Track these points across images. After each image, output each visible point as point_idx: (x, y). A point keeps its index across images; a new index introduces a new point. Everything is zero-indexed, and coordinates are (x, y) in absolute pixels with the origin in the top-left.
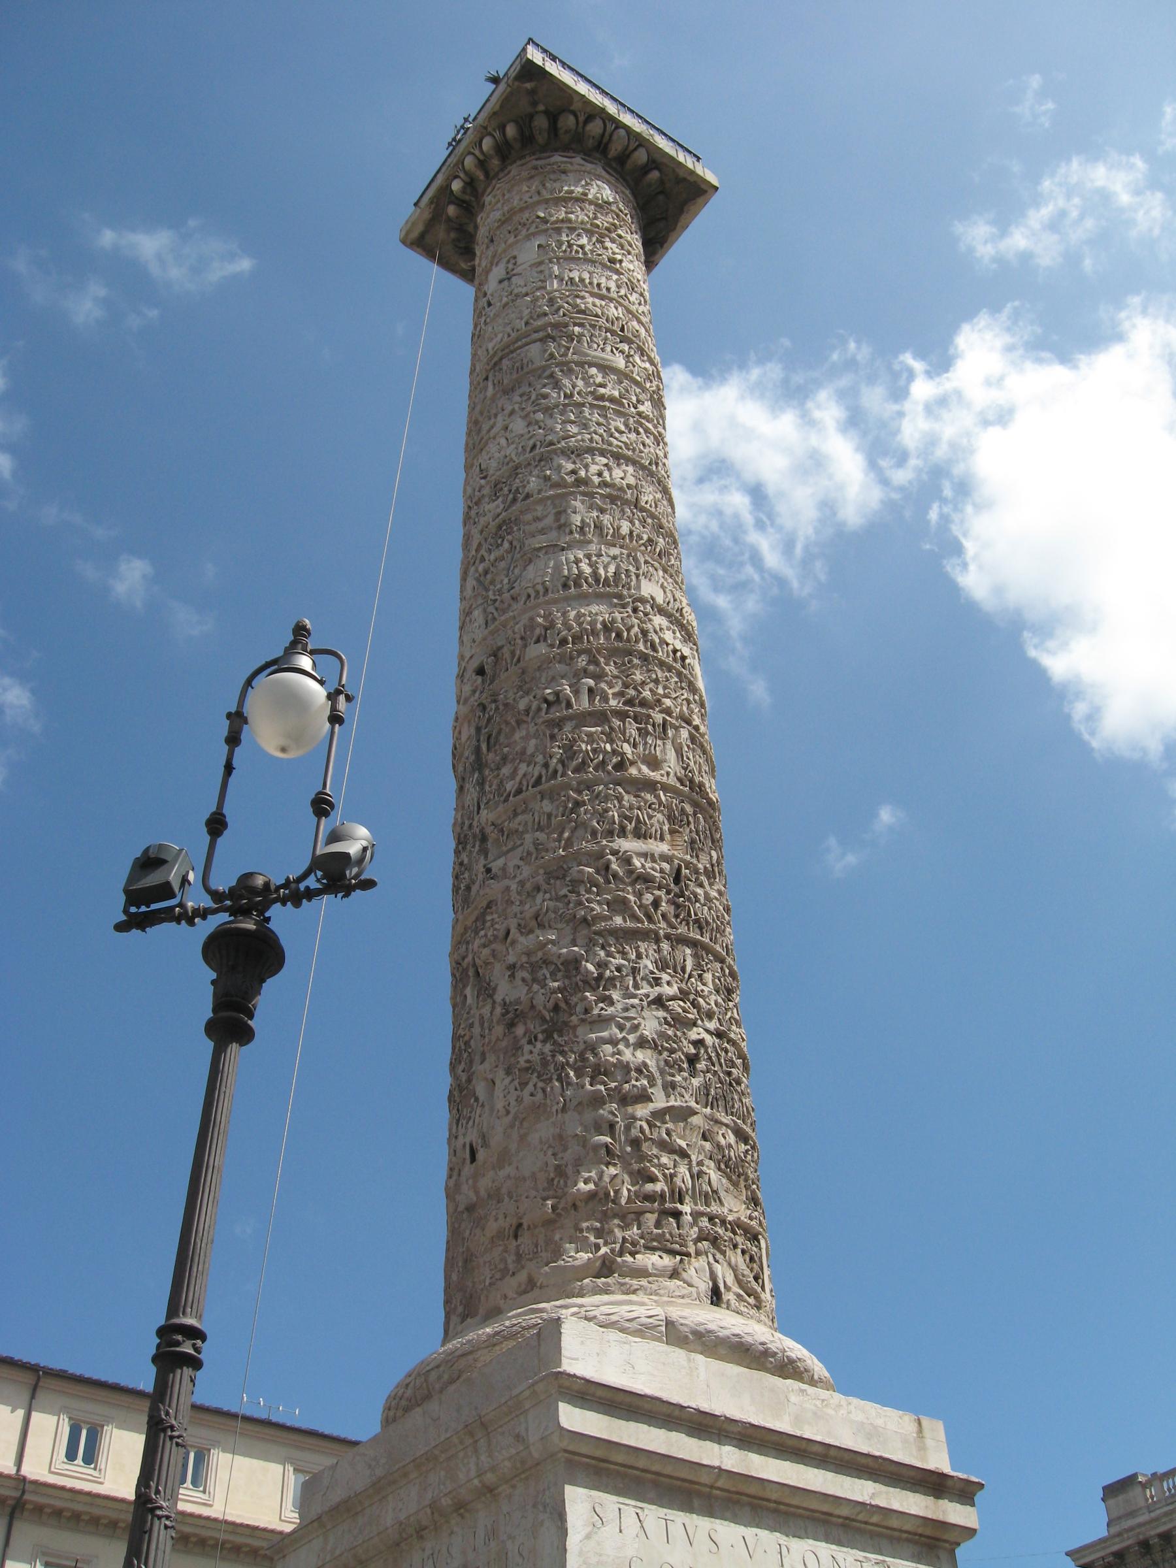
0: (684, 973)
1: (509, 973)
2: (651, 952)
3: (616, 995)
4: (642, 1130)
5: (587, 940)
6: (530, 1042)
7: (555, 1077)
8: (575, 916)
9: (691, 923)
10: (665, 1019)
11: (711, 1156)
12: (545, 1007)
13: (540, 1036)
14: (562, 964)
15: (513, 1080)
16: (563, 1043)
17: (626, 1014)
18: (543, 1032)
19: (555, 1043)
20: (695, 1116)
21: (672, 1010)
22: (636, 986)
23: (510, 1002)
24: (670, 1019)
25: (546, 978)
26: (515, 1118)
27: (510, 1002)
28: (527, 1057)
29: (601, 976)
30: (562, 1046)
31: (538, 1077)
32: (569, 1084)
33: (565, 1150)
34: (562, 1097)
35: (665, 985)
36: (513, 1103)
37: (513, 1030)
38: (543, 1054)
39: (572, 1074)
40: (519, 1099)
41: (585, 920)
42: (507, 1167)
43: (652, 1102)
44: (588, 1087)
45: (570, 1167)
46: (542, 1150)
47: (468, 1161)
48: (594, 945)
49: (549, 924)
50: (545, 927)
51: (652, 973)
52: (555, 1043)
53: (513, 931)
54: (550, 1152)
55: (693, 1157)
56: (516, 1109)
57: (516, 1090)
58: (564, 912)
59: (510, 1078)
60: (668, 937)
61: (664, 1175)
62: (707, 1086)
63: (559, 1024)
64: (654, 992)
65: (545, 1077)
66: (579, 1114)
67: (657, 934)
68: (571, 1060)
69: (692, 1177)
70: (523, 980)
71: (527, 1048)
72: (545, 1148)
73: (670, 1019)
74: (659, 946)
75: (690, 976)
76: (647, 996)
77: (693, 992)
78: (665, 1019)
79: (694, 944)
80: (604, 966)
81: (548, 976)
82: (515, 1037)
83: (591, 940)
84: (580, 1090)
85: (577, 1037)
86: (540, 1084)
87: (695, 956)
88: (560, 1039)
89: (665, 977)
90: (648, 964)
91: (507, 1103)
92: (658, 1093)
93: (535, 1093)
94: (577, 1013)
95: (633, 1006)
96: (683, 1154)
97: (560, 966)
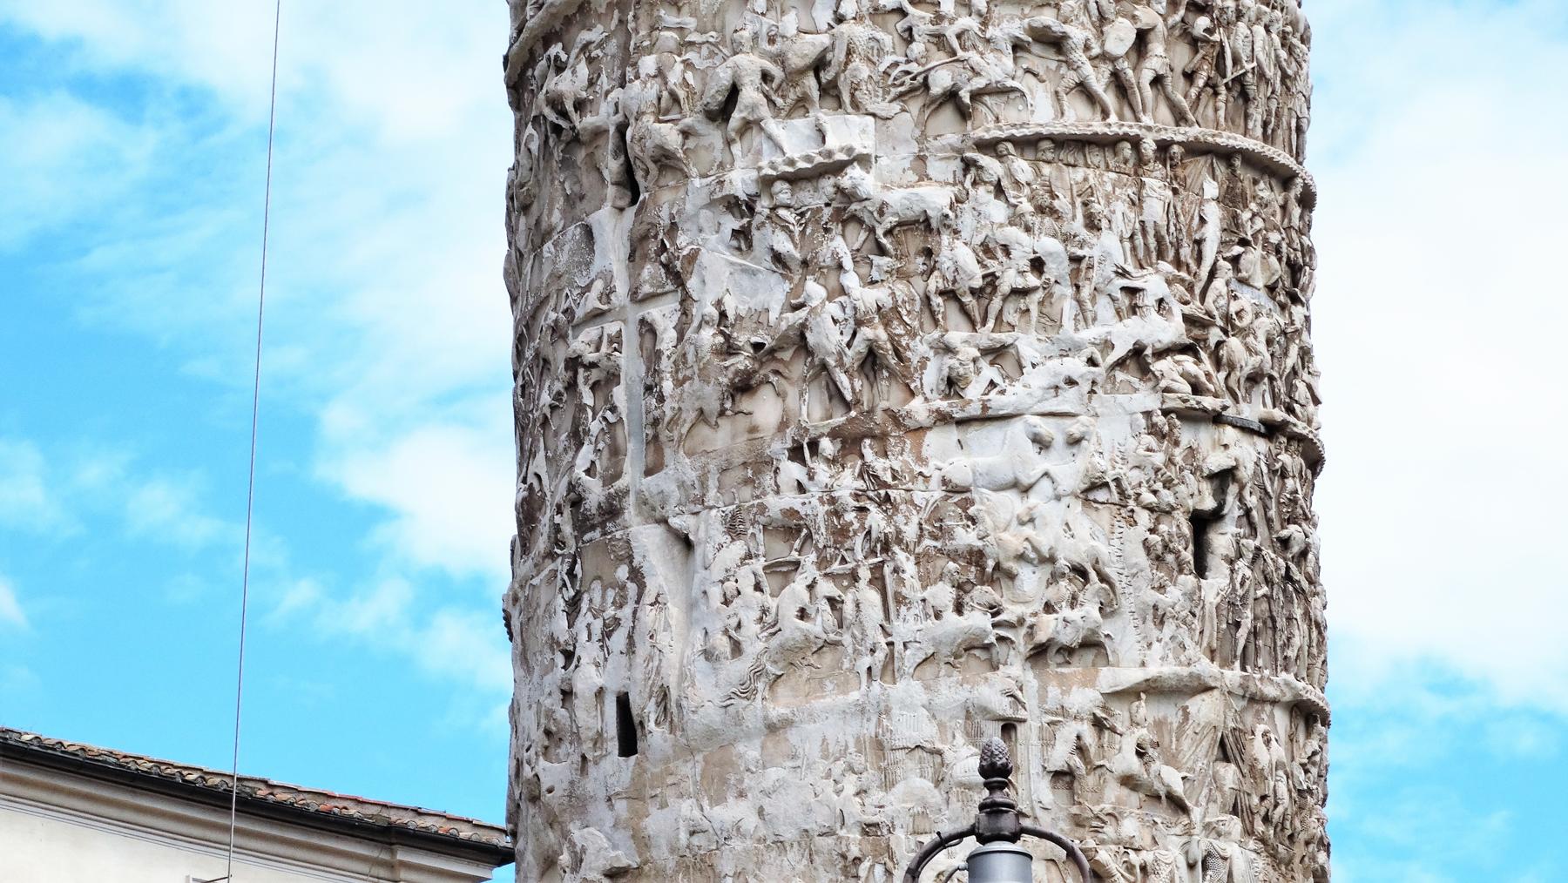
0: (1199, 259)
1: (737, 225)
2: (1121, 207)
3: (1028, 344)
4: (1081, 749)
5: (957, 165)
6: (796, 454)
7: (865, 574)
8: (926, 85)
9: (1223, 90)
10: (1148, 414)
11: (1235, 805)
12: (841, 364)
13: (827, 446)
14: (889, 233)
15: (749, 556)
16: (888, 478)
17: (1053, 405)
18: (834, 434)
19: (866, 472)
20: (1204, 696)
21: (1167, 390)
22: (1084, 316)
23: (739, 318)
24: (1159, 419)
25: (840, 267)
26: (758, 673)
27: (739, 318)
28: (790, 500)
29: (991, 280)
30: (886, 485)
31: (822, 563)
32: (901, 600)
33: (888, 784)
34: (887, 633)
35: (1154, 315)
36: (751, 628)
37: (745, 404)
38: (833, 501)
39: (910, 568)
40: (769, 619)
41: (951, 96)
42: (731, 800)
43: (1108, 664)
44: (950, 616)
45: (900, 833)
46: (828, 776)
47: (613, 746)
48: (974, 184)
49: (853, 95)
50: (838, 98)
51: (1123, 274)
52: (866, 472)
53: (750, 94)
54: (850, 784)
55: (1196, 813)
56: (760, 646)
57: (758, 587)
58: (896, 64)
59: (738, 549)
60: (1163, 147)
61: (1130, 868)
62: (1232, 604)
63: (879, 417)
64: (1126, 334)
65: (836, 567)
66: (927, 688)
67: (1136, 143)
68: (910, 533)
69: (1191, 867)
70: (778, 258)
71: (792, 471)
72: (839, 767)
73: (1159, 419)
74: (1142, 185)
75: (1212, 274)
76: (1107, 345)
77: (1220, 322)
78: (1148, 414)
79: (1226, 155)
80: (1000, 254)
81: (848, 263)
82: (753, 429)
83: (968, 165)
84: (932, 622)
85: (921, 460)
86: (826, 588)
87: (1232, 198)
88: (880, 465)
89: (1153, 283)
90: (1108, 248)
91: (733, 622)
92: (1123, 635)
93: (811, 611)
94: (927, 390)
95: (1071, 382)
96: (1178, 805)
97: (884, 241)
